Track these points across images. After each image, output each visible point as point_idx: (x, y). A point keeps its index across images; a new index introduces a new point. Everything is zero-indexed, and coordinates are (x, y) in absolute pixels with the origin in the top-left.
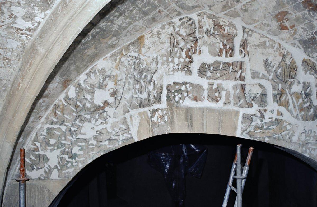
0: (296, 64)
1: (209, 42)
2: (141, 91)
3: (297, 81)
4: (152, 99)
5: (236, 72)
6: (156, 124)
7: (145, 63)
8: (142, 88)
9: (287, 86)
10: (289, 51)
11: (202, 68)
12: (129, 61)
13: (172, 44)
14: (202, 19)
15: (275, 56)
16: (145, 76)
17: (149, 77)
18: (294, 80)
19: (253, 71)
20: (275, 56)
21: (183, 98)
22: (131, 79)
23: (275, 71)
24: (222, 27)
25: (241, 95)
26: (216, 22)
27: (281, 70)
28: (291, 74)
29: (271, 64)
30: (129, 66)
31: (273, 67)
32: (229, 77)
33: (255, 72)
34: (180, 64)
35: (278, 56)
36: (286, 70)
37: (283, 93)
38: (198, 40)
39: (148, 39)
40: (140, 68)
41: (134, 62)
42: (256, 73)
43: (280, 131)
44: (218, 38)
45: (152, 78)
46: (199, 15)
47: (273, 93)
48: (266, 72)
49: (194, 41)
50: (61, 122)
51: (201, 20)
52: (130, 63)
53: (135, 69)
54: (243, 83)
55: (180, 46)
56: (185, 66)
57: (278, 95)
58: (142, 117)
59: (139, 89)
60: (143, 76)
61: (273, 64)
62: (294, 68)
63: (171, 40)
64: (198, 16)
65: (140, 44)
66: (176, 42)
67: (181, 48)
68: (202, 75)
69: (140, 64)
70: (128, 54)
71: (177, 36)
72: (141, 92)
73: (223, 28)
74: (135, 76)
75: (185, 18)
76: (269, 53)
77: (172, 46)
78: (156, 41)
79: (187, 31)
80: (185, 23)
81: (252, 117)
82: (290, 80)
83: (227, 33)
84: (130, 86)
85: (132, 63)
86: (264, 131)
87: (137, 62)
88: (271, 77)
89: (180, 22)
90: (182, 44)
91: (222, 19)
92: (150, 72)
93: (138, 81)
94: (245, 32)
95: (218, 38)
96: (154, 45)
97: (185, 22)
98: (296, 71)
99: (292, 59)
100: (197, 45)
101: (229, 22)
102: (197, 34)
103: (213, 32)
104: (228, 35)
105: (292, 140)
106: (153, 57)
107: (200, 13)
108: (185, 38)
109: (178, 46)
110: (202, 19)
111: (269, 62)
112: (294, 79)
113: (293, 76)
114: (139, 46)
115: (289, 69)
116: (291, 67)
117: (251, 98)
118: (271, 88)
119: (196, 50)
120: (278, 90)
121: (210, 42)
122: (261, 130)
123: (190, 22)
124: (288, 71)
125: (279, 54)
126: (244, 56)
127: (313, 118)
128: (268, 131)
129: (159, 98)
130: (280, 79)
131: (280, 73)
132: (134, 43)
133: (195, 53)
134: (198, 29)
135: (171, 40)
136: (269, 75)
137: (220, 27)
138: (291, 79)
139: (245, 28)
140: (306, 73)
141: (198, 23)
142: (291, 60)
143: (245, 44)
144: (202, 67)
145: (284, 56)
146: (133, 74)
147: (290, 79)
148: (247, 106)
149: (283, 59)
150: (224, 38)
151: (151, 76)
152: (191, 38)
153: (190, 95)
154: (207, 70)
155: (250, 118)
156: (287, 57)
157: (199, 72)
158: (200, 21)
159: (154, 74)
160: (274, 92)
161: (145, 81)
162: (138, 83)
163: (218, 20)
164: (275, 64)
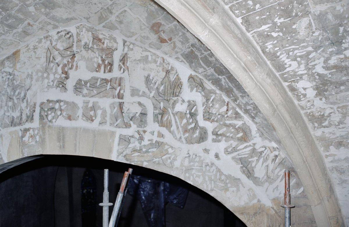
0: (181, 81)
1: (86, 57)
2: (13, 108)
3: (181, 99)
4: (24, 117)
6: (26, 144)
7: (19, 79)
8: (14, 106)
9: (170, 105)
10: (173, 66)
11: (78, 85)
12: (3, 77)
13: (48, 59)
14: (81, 32)
15: (158, 72)
16: (19, 92)
17: (22, 95)
18: (178, 99)
19: (133, 88)
20: (158, 72)
21: (57, 117)
22: (4, 96)
23: (157, 88)
24: (102, 41)
25: (118, 115)
26: (95, 36)
27: (163, 87)
28: (175, 92)
29: (153, 80)
30: (3, 82)
31: (155, 83)
32: (106, 95)
33: (134, 89)
34: (55, 80)
35: (161, 71)
36: (169, 87)
37: (165, 112)
38: (76, 55)
39: (23, 54)
40: (14, 84)
41: (9, 78)
42: (135, 90)
43: (161, 155)
44: (97, 53)
45: (25, 96)
46: (78, 28)
47: (154, 113)
48: (147, 89)
49: (71, 56)
51: (79, 33)
52: (4, 79)
53: (8, 85)
55: (57, 61)
56: (61, 83)
57: (159, 114)
58: (13, 137)
59: (12, 107)
60: (17, 93)
61: (155, 81)
62: (179, 85)
63: (47, 55)
64: (77, 29)
65: (15, 59)
66: (53, 57)
67: (57, 63)
69: (14, 80)
70: (3, 70)
71: (54, 50)
72: (13, 109)
73: (102, 42)
74: (8, 93)
75: (64, 31)
76: (151, 69)
77: (48, 61)
78: (31, 55)
79: (64, 46)
80: (63, 37)
81: (129, 138)
82: (173, 98)
83: (106, 47)
84: (2, 104)
85: (6, 79)
86: (142, 155)
87: (11, 78)
88: (152, 95)
89: (58, 35)
90: (58, 59)
91: (101, 32)
92: (23, 88)
93: (10, 98)
94: (126, 46)
95: (97, 53)
96: (30, 60)
97: (63, 35)
98: (181, 89)
99: (177, 75)
100: (74, 60)
101: (109, 34)
102: (75, 49)
103: (92, 45)
104: (108, 49)
105: (174, 165)
106: (28, 72)
107: (79, 26)
108: (62, 52)
109: (54, 61)
110: (81, 32)
111: (151, 78)
112: (178, 97)
113: (177, 94)
114: (15, 61)
115: (173, 86)
117: (129, 117)
118: (152, 106)
119: (72, 66)
120: (159, 109)
121: (89, 57)
122: (139, 153)
123: (68, 36)
124: (171, 88)
125: (162, 69)
126: (124, 72)
127: (199, 141)
128: (147, 155)
129: (31, 117)
130: (162, 97)
131: (162, 90)
132: (9, 58)
133: (71, 68)
134: (76, 43)
135: (47, 55)
136: (150, 93)
137: (100, 40)
138: (175, 97)
139: (126, 42)
140: (192, 90)
141: (77, 36)
142: (176, 76)
143: (125, 58)
144: (78, 83)
145: (168, 72)
146: (7, 90)
147: (173, 97)
148: (124, 126)
149: (166, 75)
150: (103, 52)
151: (24, 93)
152: (69, 53)
153: (64, 114)
154: (83, 87)
155: (127, 140)
156: (171, 72)
157: (75, 88)
158: (78, 34)
159: (27, 91)
160: (155, 111)
161: (18, 98)
162: (11, 100)
163: (97, 33)
164: (158, 80)
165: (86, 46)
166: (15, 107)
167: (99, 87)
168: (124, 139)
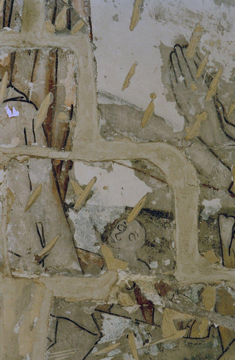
5: (31, 102)
25: (47, 216)
33: (118, 106)
42: (122, 108)
47: (201, 209)
48: (175, 103)
54: (64, 155)
57: (226, 216)
117: (95, 228)
126: (69, 27)
148: (75, 266)
160: (205, 203)
168: (77, 321)
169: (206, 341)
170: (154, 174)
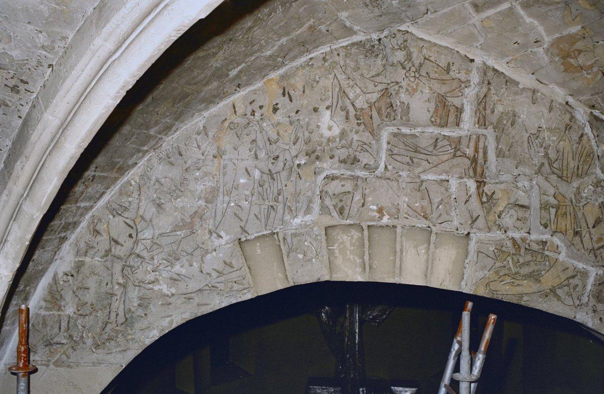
2: (268, 193)
5: (467, 157)
11: (396, 148)
36: (571, 155)
50: (103, 253)
57: (553, 207)
68: (396, 161)
116: (583, 150)
124: (574, 159)
165: (411, 72)
166: (272, 190)
167: (438, 154)
169: (544, 263)
170: (521, 189)
